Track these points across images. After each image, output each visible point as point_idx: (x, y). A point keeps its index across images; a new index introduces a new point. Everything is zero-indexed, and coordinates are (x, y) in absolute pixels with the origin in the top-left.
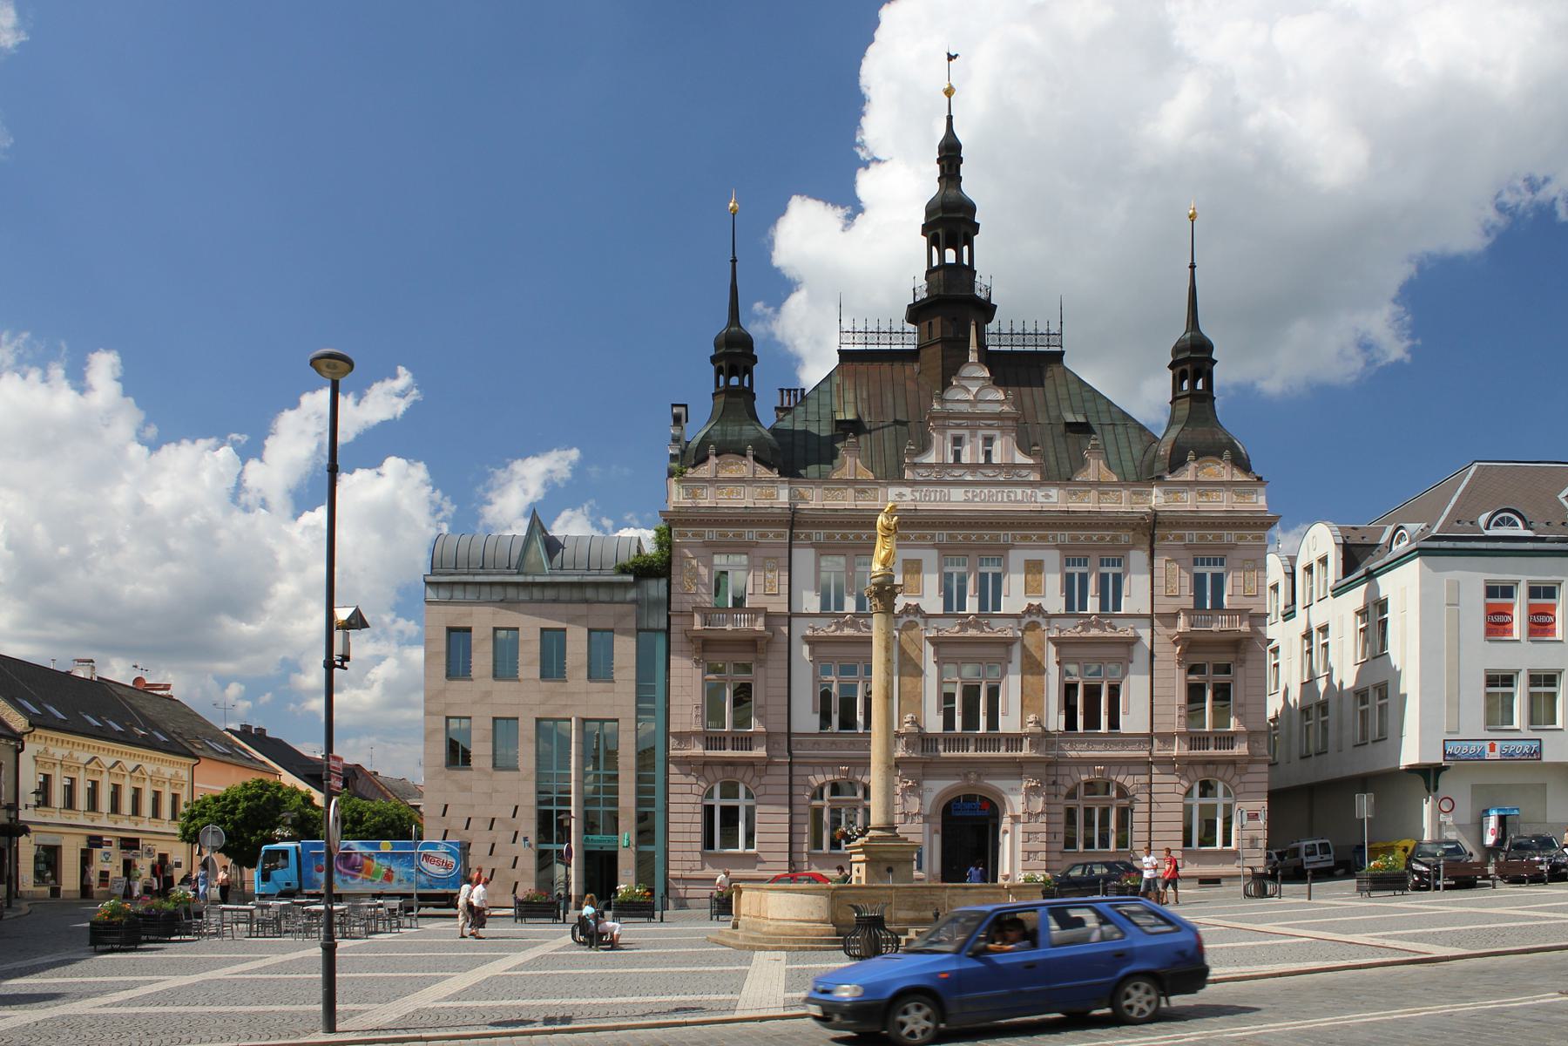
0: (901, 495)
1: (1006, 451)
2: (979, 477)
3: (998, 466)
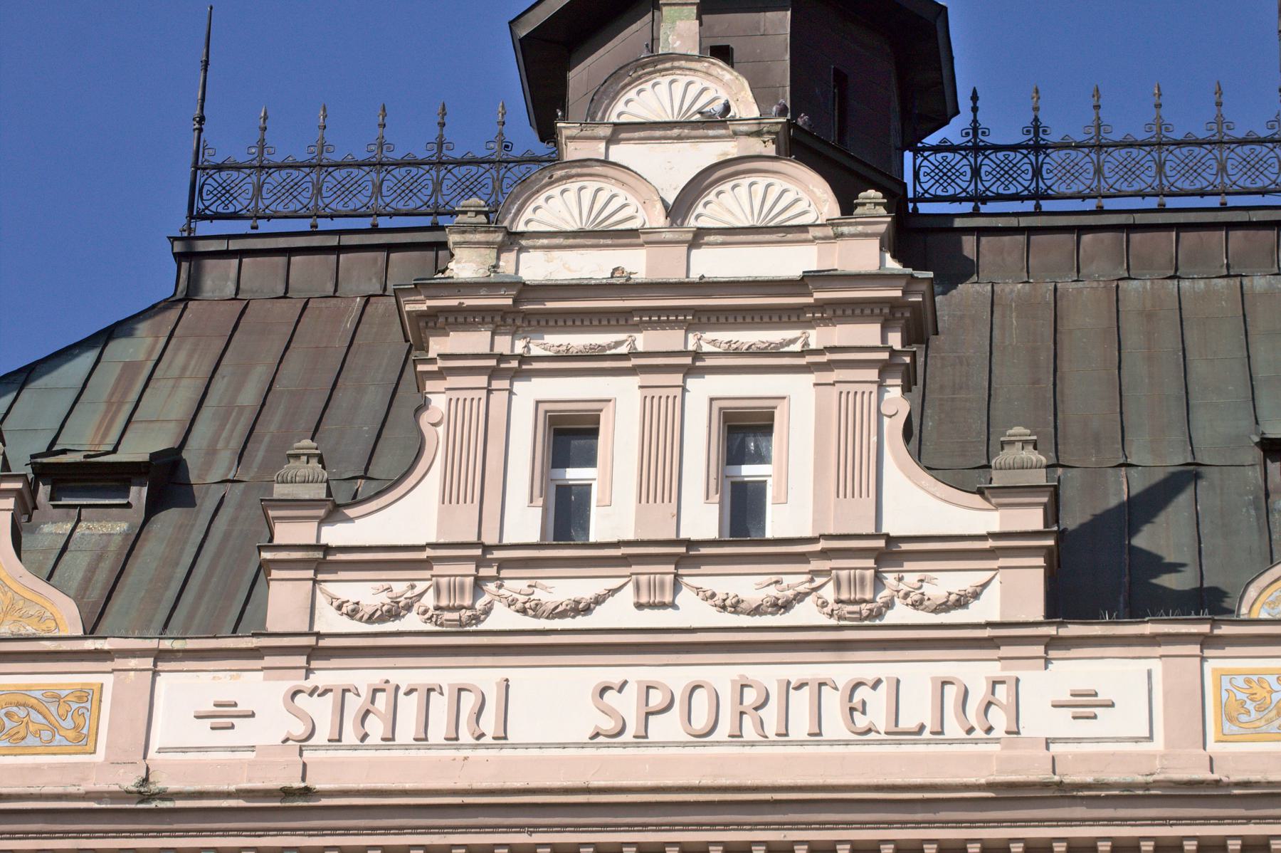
0: (224, 715)
1: (854, 472)
2: (692, 610)
3: (790, 552)
